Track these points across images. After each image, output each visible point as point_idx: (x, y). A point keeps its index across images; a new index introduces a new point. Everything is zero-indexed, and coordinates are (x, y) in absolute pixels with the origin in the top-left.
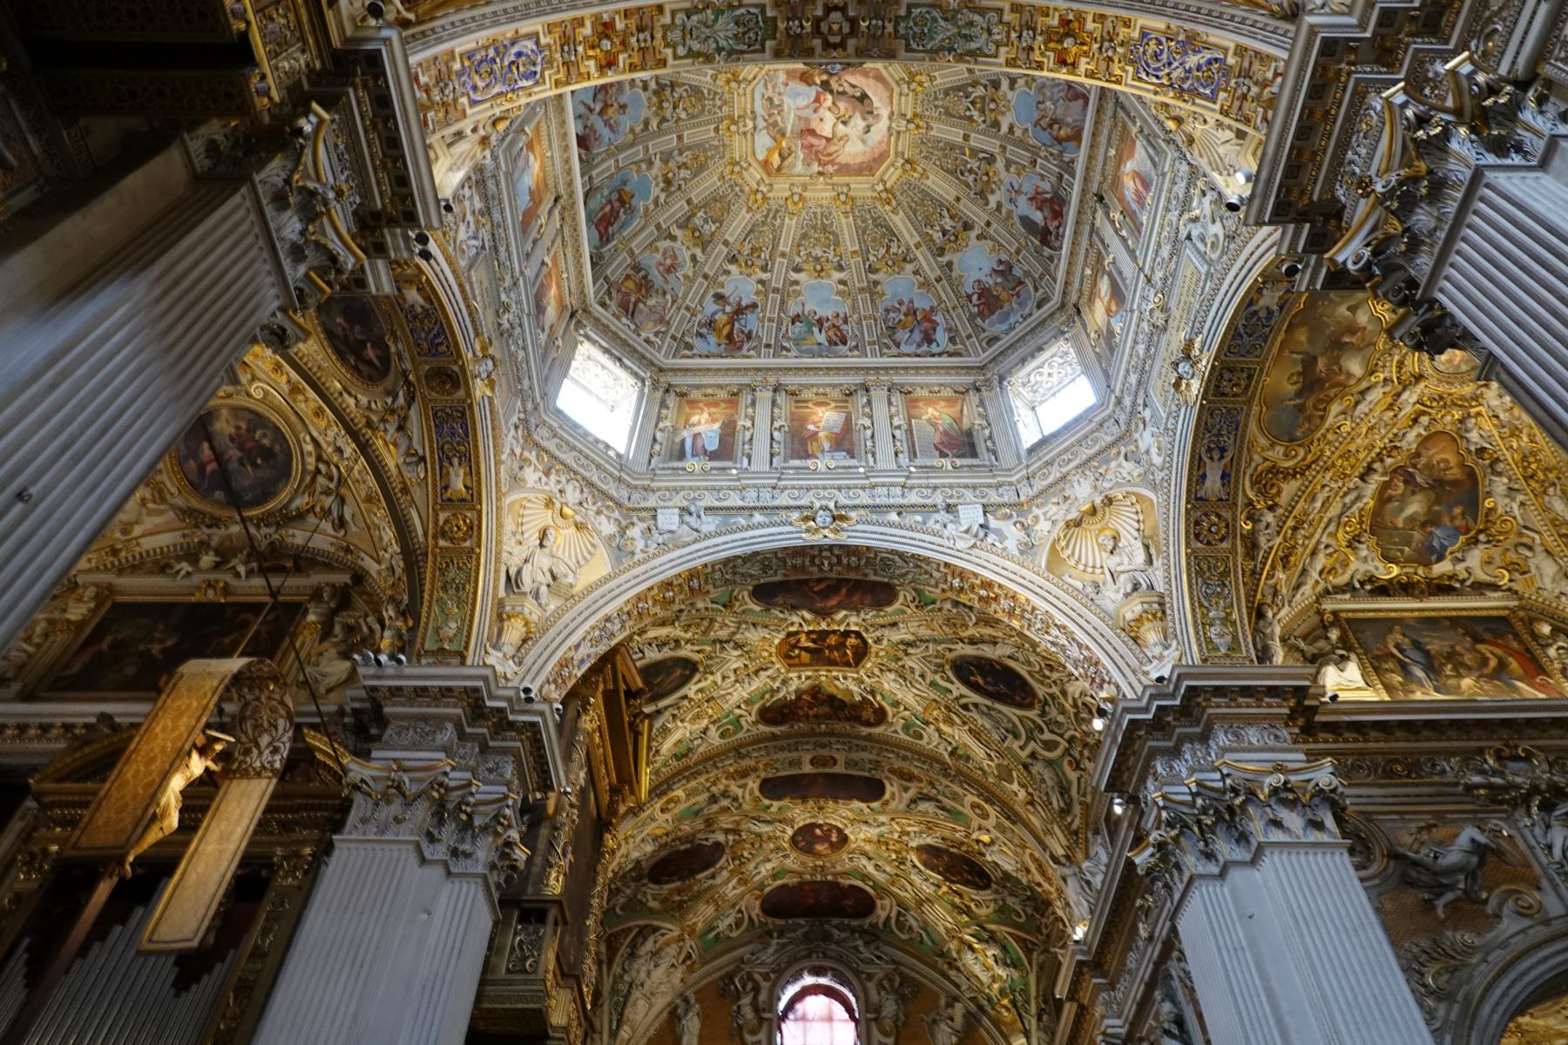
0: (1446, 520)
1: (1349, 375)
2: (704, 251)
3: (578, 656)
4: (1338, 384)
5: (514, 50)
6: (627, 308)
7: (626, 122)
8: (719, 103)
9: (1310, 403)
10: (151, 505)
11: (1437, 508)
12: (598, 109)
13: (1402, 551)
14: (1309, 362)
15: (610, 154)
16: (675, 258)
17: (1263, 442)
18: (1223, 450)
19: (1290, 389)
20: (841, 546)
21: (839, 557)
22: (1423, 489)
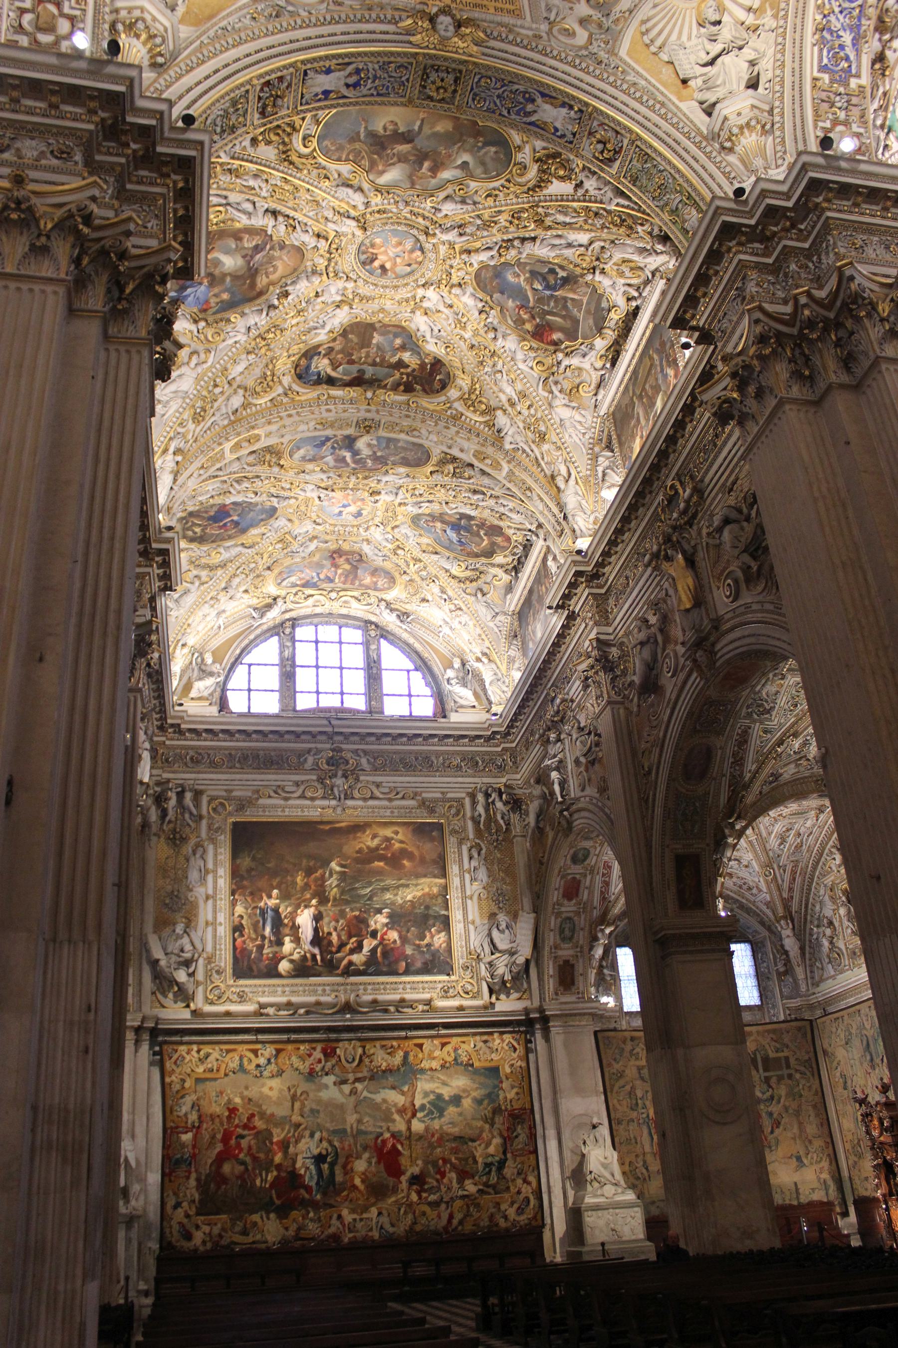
0: (216, 290)
1: (382, 173)
4: (373, 164)
11: (228, 279)
14: (407, 138)
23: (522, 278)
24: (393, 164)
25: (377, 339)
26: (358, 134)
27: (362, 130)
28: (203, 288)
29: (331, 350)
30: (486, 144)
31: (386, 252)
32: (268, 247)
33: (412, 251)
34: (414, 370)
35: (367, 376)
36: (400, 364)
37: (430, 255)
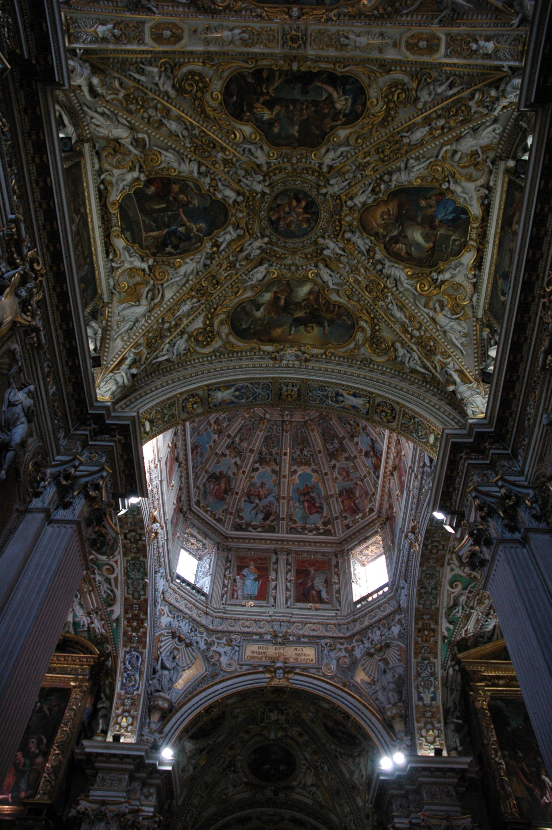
0: (430, 211)
1: (311, 292)
2: (345, 452)
3: (427, 701)
4: (317, 299)
5: (127, 663)
6: (355, 511)
7: (269, 484)
8: (275, 427)
9: (329, 316)
10: (357, 761)
11: (419, 219)
12: (257, 501)
13: (455, 241)
15: (278, 500)
16: (344, 468)
17: (352, 345)
18: (338, 394)
19: (317, 330)
20: (426, 538)
21: (433, 542)
22: (403, 231)
23: (195, 229)
24: (304, 300)
25: (295, 130)
26: (329, 326)
27: (327, 328)
28: (440, 217)
29: (335, 118)
30: (249, 328)
31: (298, 215)
32: (387, 239)
33: (279, 219)
34: (258, 100)
35: (299, 86)
36: (270, 105)
37: (265, 223)
